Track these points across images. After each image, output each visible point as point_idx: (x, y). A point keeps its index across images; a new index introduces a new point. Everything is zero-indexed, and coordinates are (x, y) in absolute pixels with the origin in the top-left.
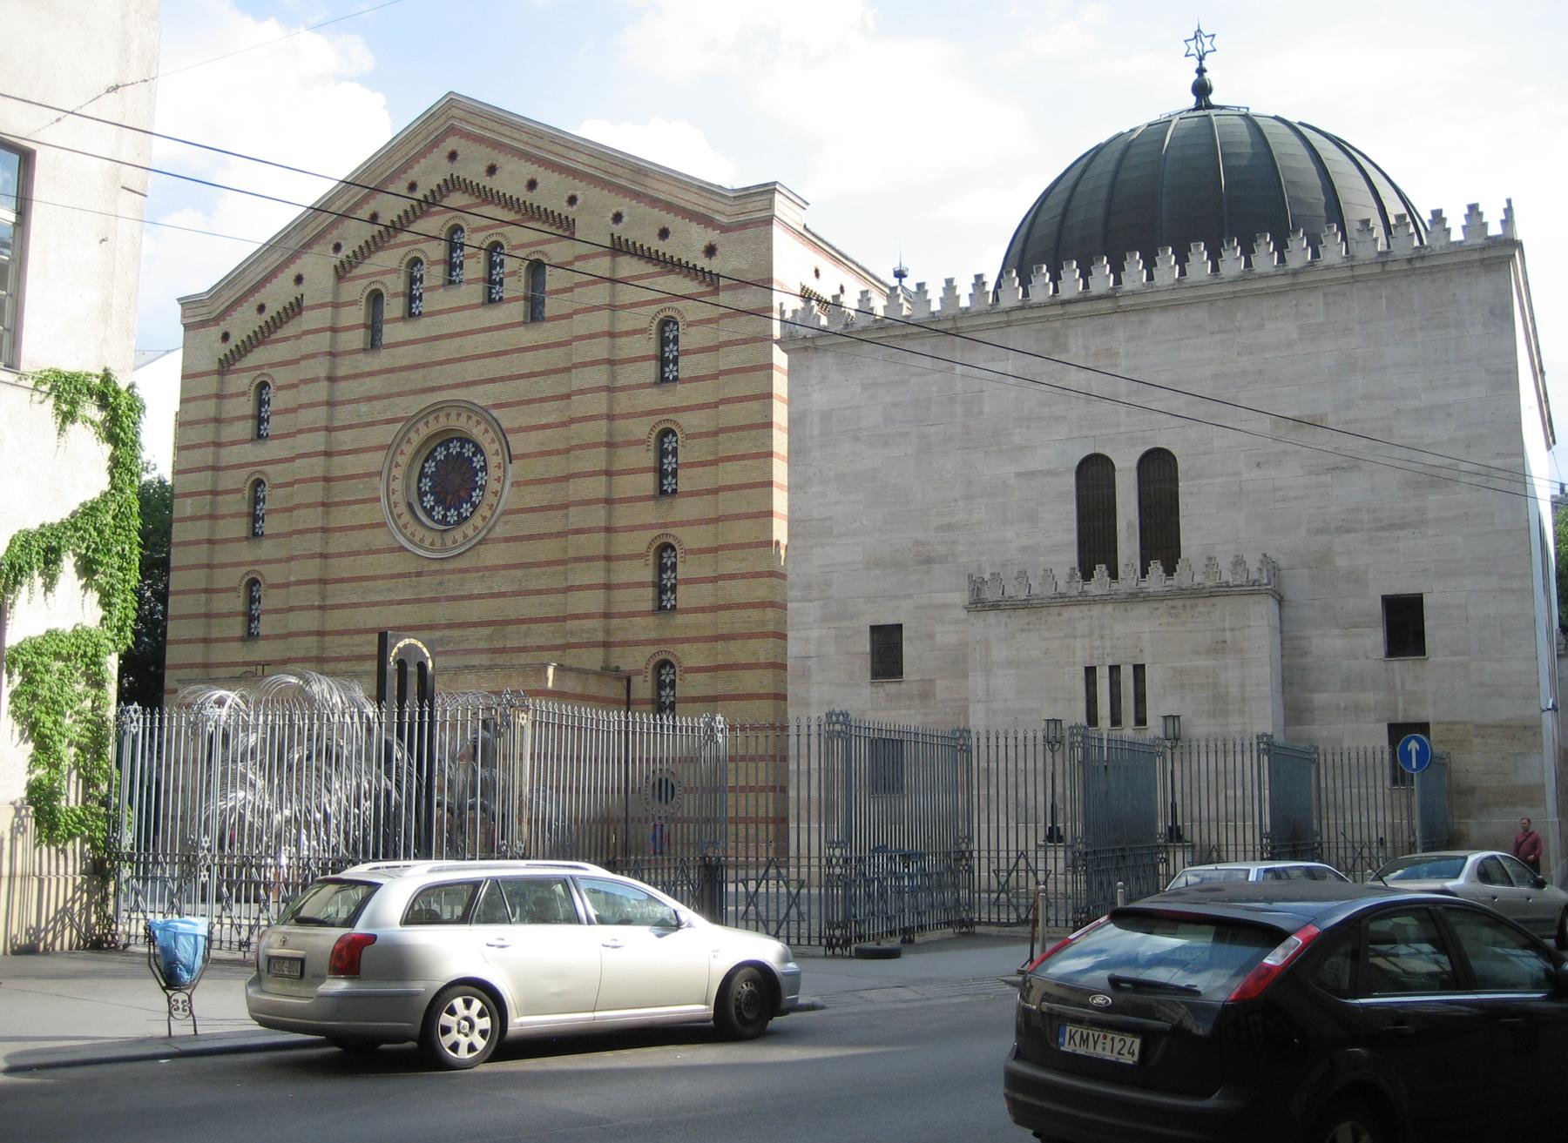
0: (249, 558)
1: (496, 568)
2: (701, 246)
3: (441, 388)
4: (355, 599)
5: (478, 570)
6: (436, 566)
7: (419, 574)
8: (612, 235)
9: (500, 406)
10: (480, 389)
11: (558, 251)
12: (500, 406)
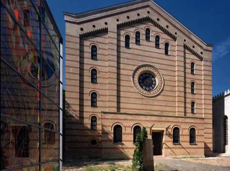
0: (93, 87)
1: (161, 100)
2: (200, 52)
3: (146, 62)
4: (126, 101)
5: (157, 100)
6: (146, 98)
7: (143, 99)
8: (184, 43)
9: (160, 69)
10: (155, 64)
11: (171, 42)
12: (160, 69)
